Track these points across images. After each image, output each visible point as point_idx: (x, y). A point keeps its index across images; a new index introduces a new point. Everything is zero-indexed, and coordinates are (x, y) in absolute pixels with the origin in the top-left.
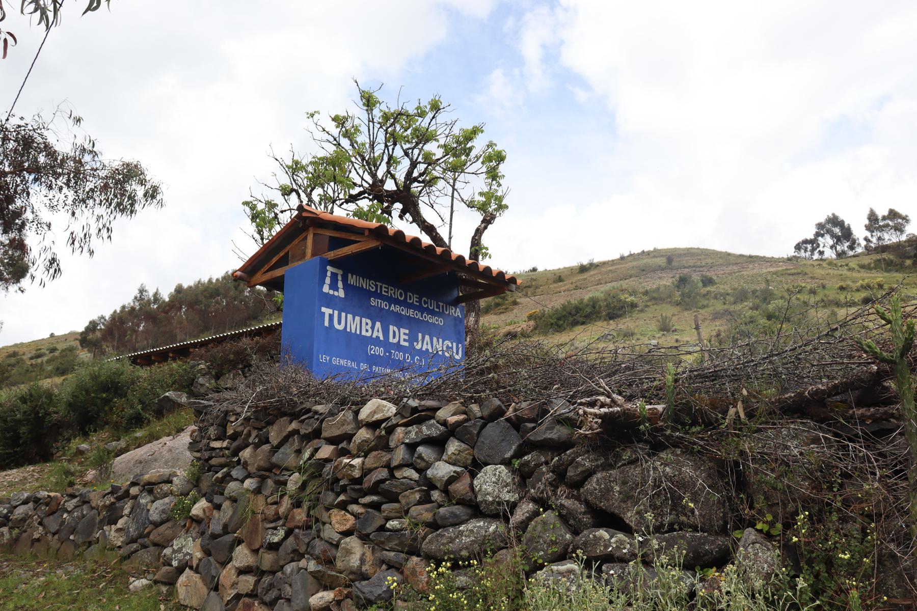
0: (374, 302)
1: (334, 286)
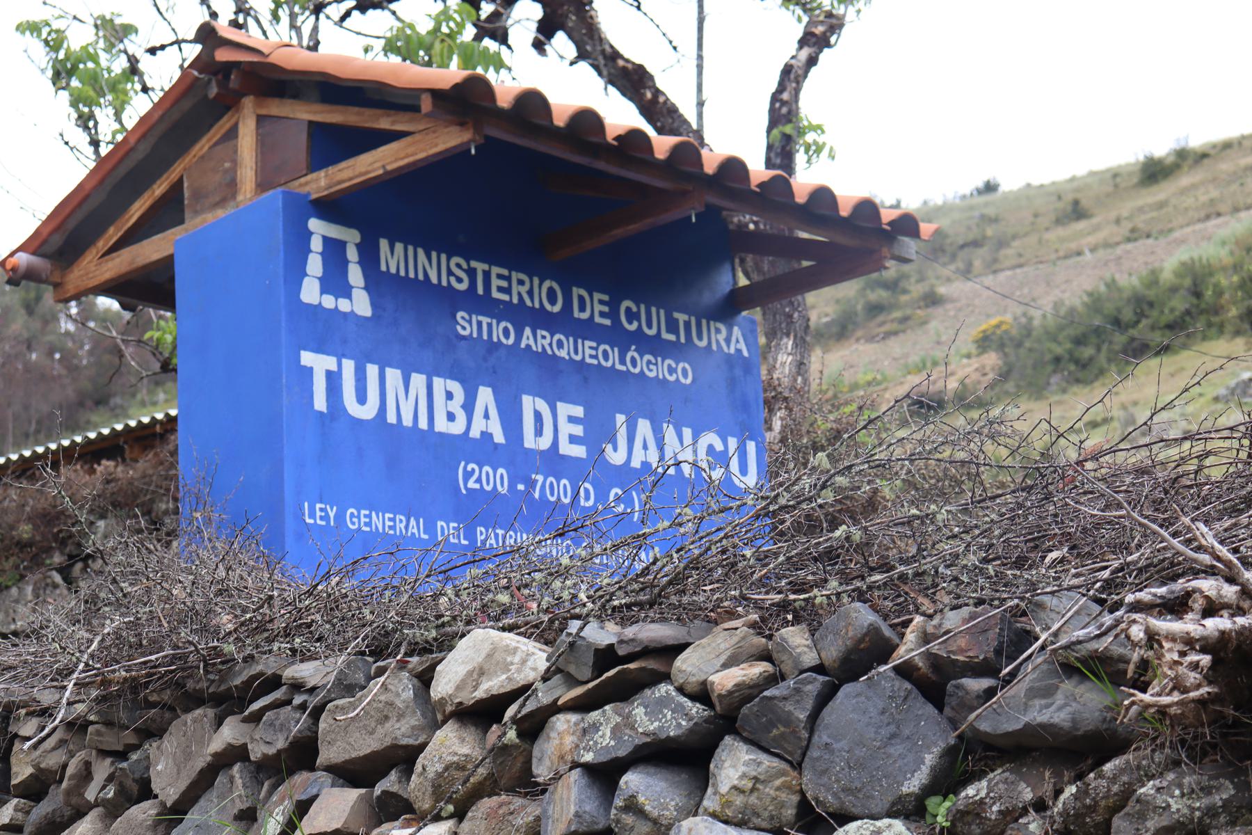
0: (466, 324)
1: (335, 282)
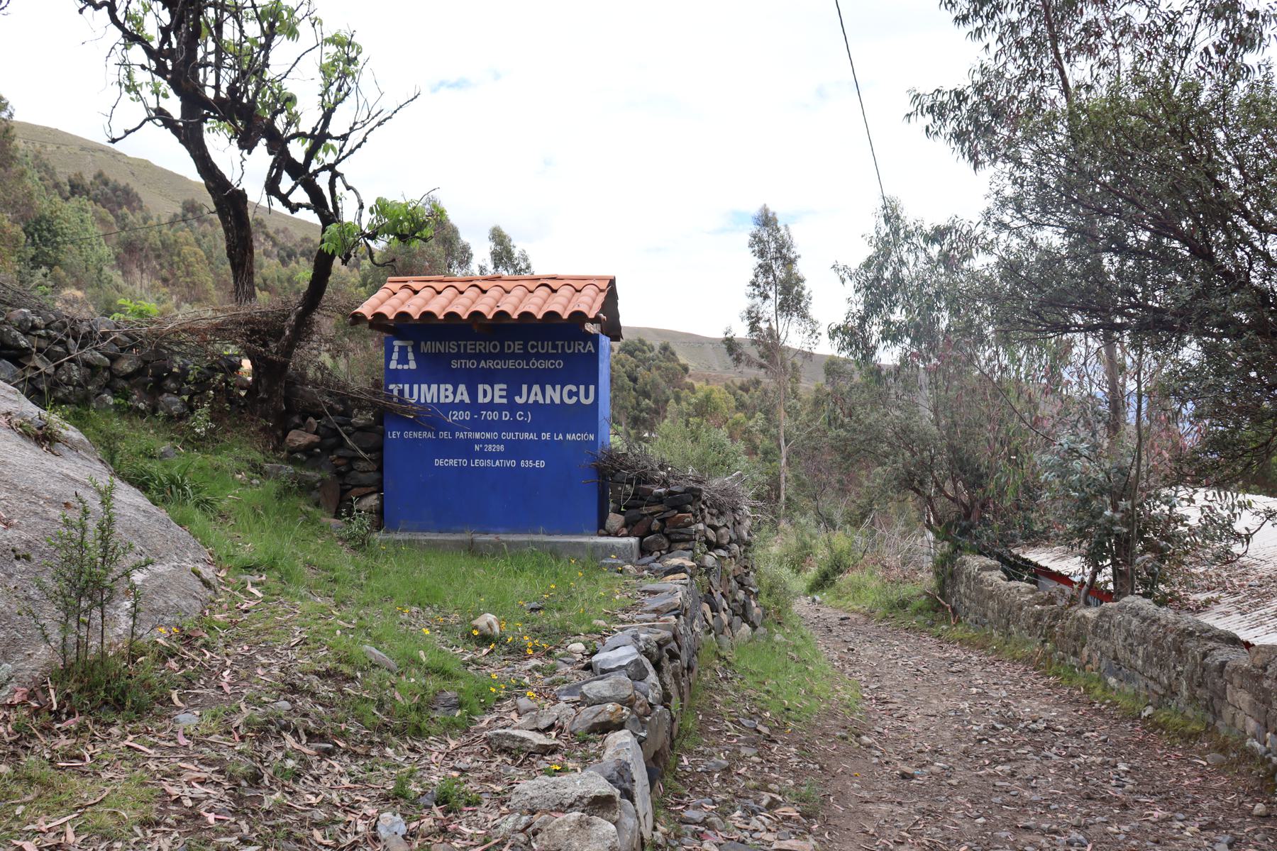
0: (455, 364)
1: (403, 359)
